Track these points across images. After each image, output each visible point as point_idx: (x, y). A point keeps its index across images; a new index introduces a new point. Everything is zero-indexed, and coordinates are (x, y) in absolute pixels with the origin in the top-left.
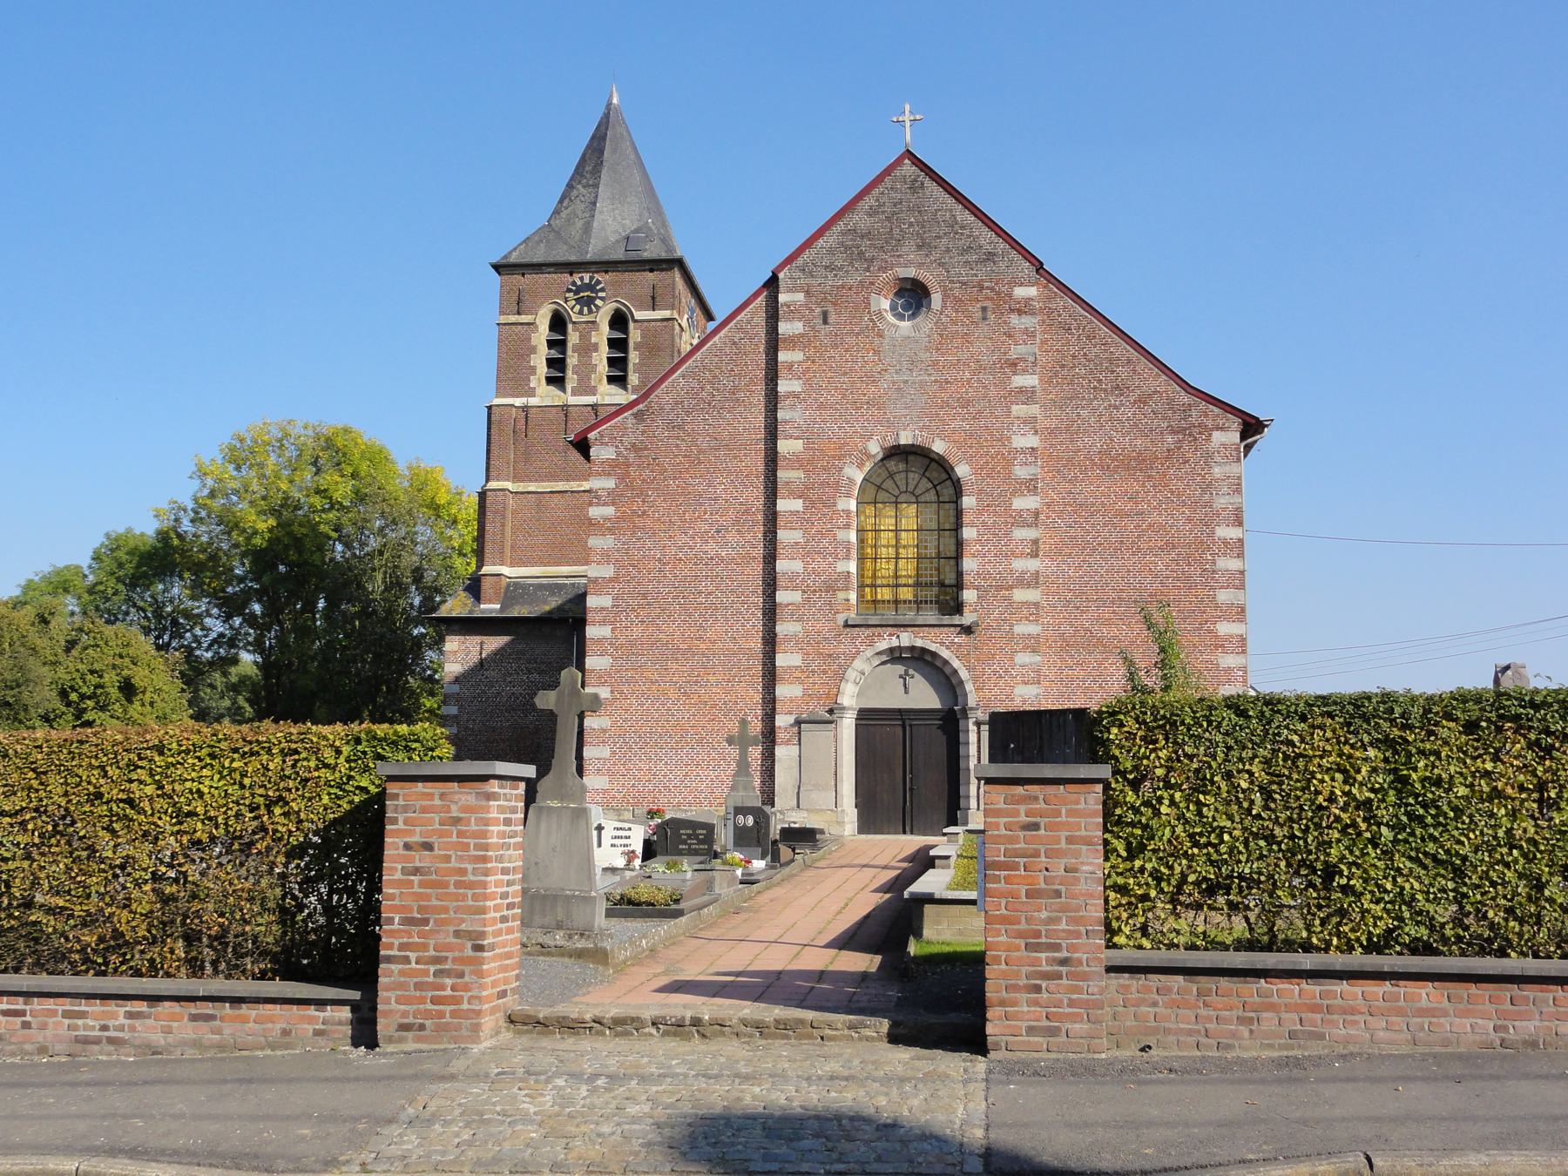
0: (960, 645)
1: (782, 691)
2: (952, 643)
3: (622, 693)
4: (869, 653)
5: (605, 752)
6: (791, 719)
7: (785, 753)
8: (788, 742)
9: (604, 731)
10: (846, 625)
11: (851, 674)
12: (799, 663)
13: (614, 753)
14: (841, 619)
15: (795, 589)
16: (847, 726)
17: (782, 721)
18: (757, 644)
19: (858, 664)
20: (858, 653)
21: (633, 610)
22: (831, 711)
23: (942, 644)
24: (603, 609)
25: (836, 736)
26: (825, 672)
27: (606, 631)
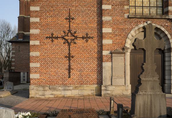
0: (167, 26)
1: (105, 42)
2: (165, 25)
3: (44, 43)
4: (136, 28)
5: (38, 65)
6: (108, 52)
7: (107, 65)
8: (107, 61)
9: (37, 57)
10: (128, 17)
11: (130, 36)
12: (111, 32)
13: (41, 65)
14: (126, 15)
15: (109, 4)
16: (128, 54)
17: (105, 53)
18: (95, 25)
19: (132, 32)
20: (132, 28)
21: (48, 12)
22: (123, 49)
23: (161, 25)
24: (36, 11)
25: (125, 59)
26: (120, 35)
27: (37, 20)
